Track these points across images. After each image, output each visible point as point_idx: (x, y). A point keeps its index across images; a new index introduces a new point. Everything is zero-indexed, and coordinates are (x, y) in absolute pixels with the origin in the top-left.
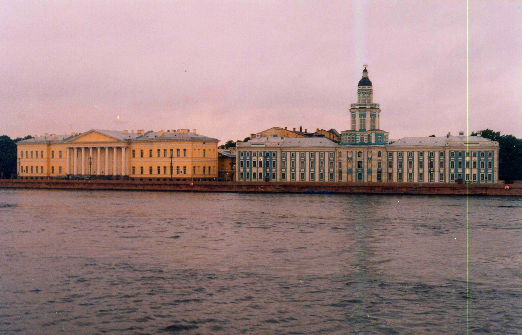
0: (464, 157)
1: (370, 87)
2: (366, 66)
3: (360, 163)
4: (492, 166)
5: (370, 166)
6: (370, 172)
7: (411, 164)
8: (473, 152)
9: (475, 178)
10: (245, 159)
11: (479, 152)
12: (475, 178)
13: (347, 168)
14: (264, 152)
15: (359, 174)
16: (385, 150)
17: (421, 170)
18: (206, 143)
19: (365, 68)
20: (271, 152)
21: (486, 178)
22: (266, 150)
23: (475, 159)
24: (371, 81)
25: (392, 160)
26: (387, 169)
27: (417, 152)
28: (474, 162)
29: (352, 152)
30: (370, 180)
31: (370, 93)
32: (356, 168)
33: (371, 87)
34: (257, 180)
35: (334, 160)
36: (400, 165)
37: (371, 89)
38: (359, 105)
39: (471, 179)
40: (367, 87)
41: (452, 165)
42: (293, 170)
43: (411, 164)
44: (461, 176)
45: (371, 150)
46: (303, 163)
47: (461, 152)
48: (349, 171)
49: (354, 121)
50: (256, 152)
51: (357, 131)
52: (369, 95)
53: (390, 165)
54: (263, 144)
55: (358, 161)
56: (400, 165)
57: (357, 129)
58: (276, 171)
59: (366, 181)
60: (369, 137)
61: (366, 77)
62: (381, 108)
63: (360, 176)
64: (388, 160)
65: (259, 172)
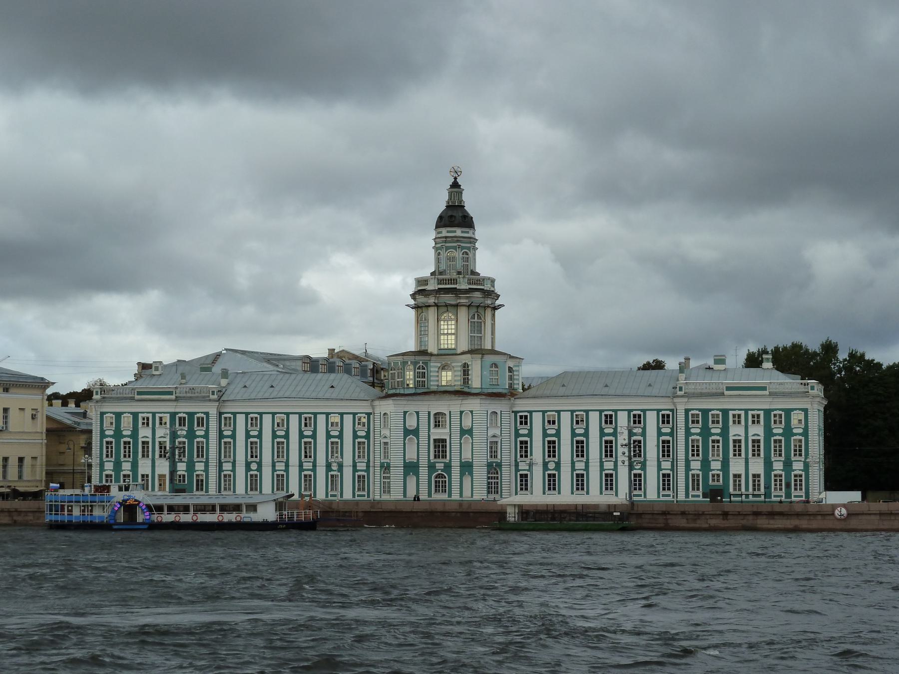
1: (468, 232)
2: (456, 173)
3: (440, 446)
4: (642, 454)
5: (467, 456)
6: (467, 467)
7: (580, 449)
8: (750, 413)
9: (756, 486)
10: (118, 434)
11: (767, 412)
12: (756, 486)
13: (404, 460)
14: (173, 415)
15: (436, 477)
16: (511, 408)
17: (609, 465)
18: (11, 390)
19: (456, 178)
20: (191, 415)
21: (788, 485)
22: (177, 411)
23: (757, 431)
24: (472, 215)
25: (530, 434)
26: (516, 460)
28: (754, 441)
29: (417, 413)
30: (467, 494)
31: (469, 248)
32: (429, 460)
33: (471, 231)
35: (367, 436)
36: (552, 449)
37: (470, 238)
39: (747, 489)
40: (459, 232)
41: (693, 450)
42: (254, 466)
43: (580, 449)
44: (718, 481)
46: (281, 449)
47: (718, 412)
48: (411, 468)
50: (150, 416)
51: (431, 355)
52: (467, 254)
53: (524, 448)
54: (170, 393)
55: (435, 440)
56: (552, 449)
57: (432, 349)
58: (206, 470)
59: (455, 496)
60: (466, 370)
62: (498, 289)
63: (441, 483)
64: (517, 435)
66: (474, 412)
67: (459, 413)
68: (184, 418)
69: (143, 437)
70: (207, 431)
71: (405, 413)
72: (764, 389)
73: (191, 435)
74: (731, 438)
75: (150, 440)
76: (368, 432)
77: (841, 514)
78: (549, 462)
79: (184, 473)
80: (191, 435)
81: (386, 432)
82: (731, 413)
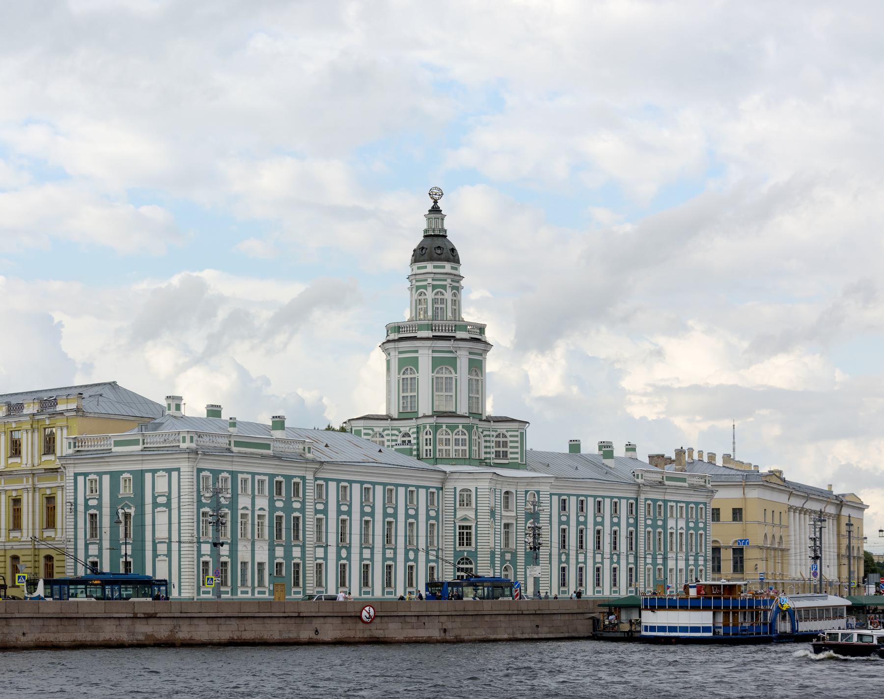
0: (665, 521)
1: (456, 269)
2: (435, 195)
14: (272, 476)
19: (436, 202)
20: (289, 478)
27: (593, 498)
34: (253, 594)
35: (436, 518)
38: (431, 328)
45: (537, 488)
49: (408, 385)
50: (249, 476)
58: (303, 557)
61: (437, 233)
65: (258, 559)
66: (541, 493)
67: (524, 493)
68: (280, 482)
69: (243, 509)
70: (303, 503)
71: (491, 488)
72: (684, 480)
73: (288, 508)
74: (669, 531)
75: (249, 512)
76: (437, 512)
77: (370, 616)
78: (563, 553)
79: (281, 561)
80: (288, 508)
81: (471, 514)
82: (669, 504)
